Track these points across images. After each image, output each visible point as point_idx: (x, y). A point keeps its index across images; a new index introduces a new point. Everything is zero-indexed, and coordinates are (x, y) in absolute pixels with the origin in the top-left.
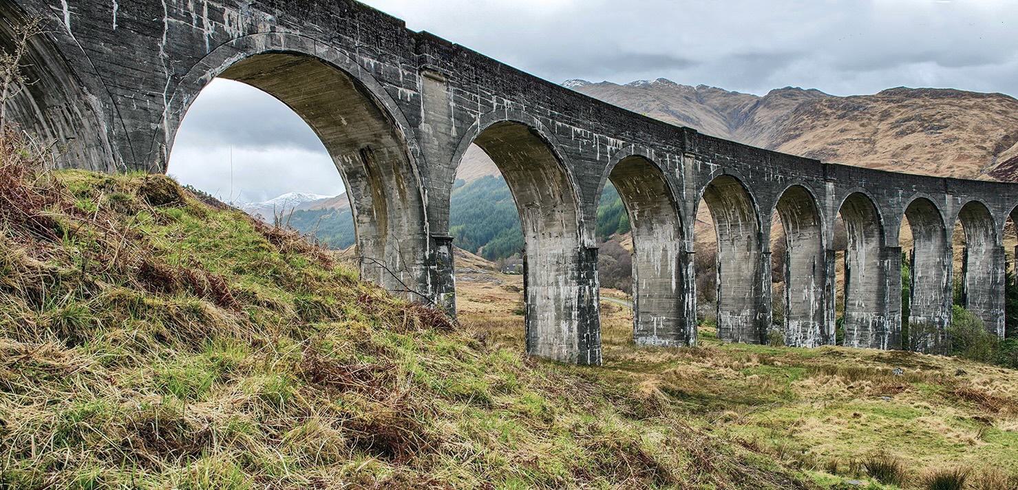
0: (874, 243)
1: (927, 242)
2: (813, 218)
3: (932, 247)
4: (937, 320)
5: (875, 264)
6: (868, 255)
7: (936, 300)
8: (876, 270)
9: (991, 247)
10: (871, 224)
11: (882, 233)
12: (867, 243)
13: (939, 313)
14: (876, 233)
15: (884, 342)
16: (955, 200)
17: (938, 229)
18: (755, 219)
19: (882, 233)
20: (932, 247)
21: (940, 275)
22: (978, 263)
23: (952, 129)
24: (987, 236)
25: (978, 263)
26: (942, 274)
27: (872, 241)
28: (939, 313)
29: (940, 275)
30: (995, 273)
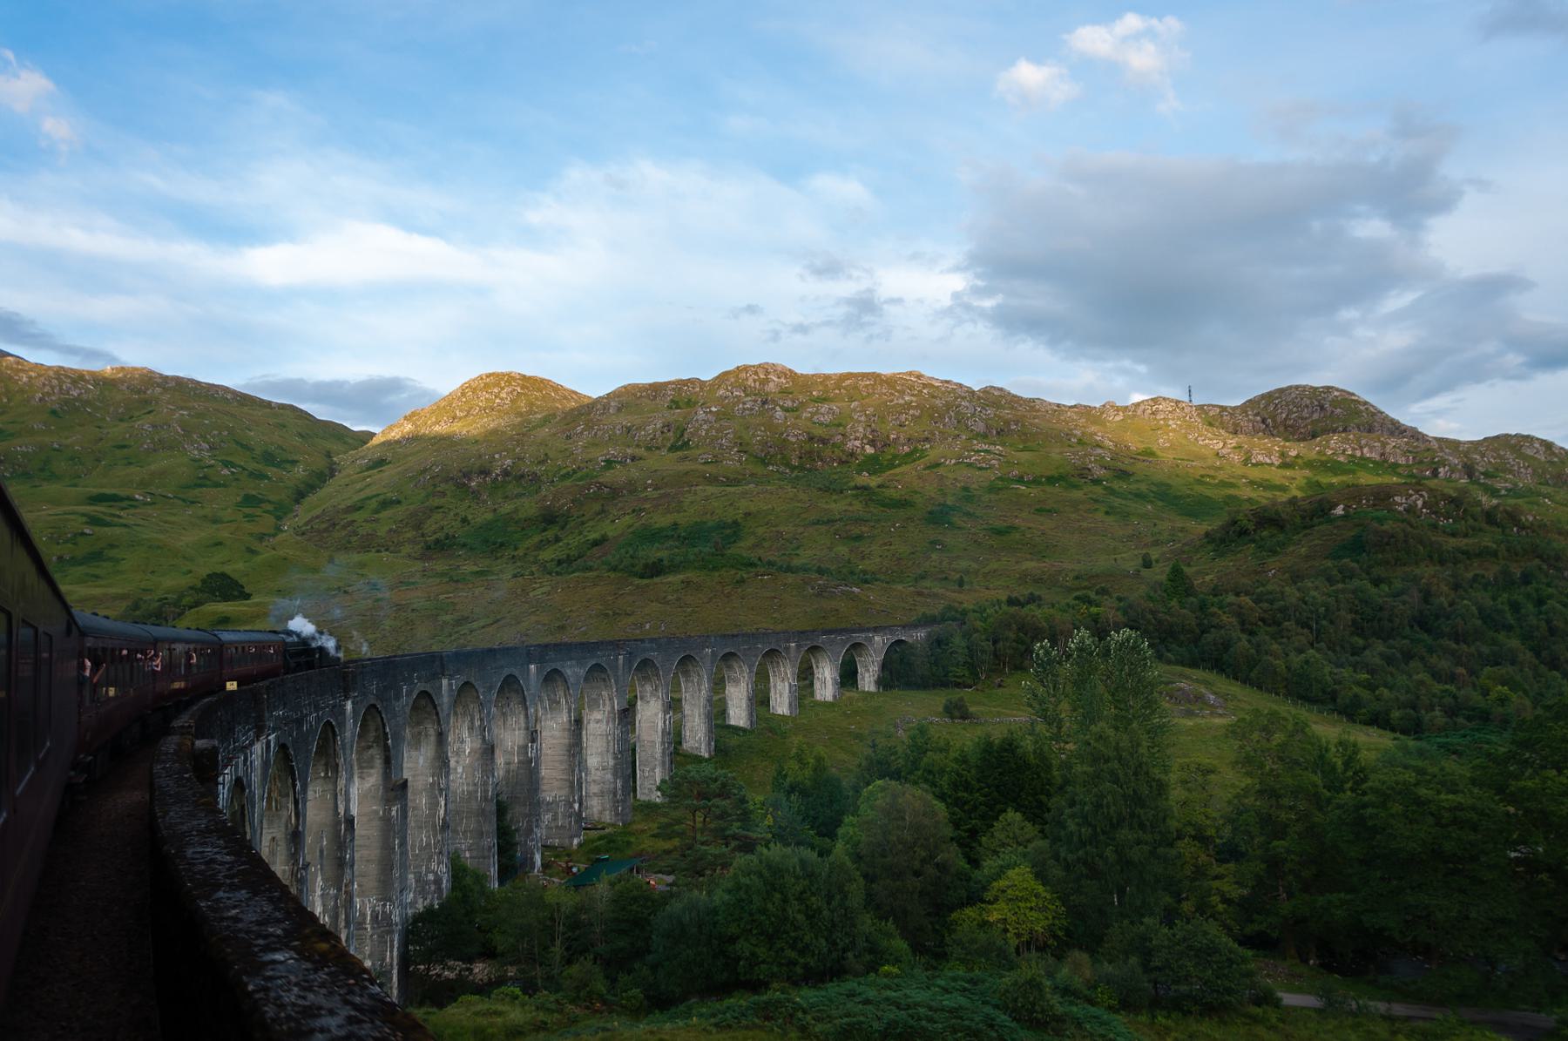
0: (373, 779)
1: (414, 753)
2: (326, 765)
3: (421, 761)
4: (431, 877)
5: (376, 812)
6: (363, 797)
7: (428, 844)
8: (376, 823)
9: (478, 744)
10: (370, 747)
12: (361, 778)
13: (434, 866)
14: (378, 762)
15: (392, 947)
16: (450, 685)
17: (432, 732)
18: (291, 806)
19: (387, 761)
20: (421, 761)
21: (434, 805)
22: (460, 770)
24: (471, 728)
25: (460, 770)
26: (438, 804)
27: (370, 775)
28: (434, 866)
29: (434, 805)
30: (485, 784)
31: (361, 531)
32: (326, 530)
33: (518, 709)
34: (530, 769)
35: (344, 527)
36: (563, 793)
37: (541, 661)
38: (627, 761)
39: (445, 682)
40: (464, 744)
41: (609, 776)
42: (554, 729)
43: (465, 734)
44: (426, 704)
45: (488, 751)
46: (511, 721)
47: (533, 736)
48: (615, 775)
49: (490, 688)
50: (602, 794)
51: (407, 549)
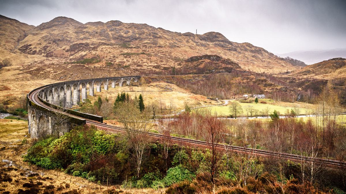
9: (57, 95)
11: (47, 98)
14: (46, 98)
23: (2, 30)
31: (33, 50)
32: (25, 49)
33: (63, 90)
34: (65, 98)
35: (29, 49)
36: (70, 101)
37: (66, 84)
38: (79, 97)
39: (53, 88)
40: (56, 96)
41: (77, 99)
42: (68, 93)
43: (56, 94)
44: (51, 91)
45: (59, 96)
46: (62, 92)
47: (65, 94)
48: (78, 99)
49: (59, 88)
50: (76, 101)
51: (43, 54)
